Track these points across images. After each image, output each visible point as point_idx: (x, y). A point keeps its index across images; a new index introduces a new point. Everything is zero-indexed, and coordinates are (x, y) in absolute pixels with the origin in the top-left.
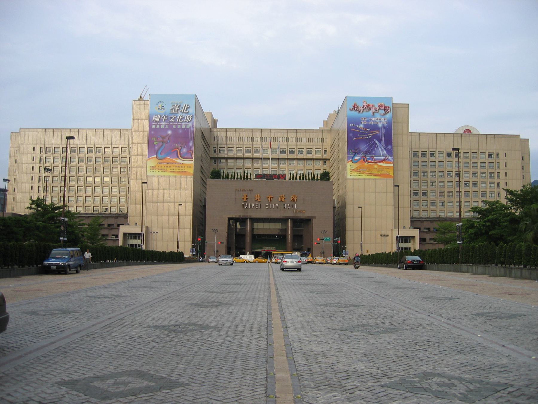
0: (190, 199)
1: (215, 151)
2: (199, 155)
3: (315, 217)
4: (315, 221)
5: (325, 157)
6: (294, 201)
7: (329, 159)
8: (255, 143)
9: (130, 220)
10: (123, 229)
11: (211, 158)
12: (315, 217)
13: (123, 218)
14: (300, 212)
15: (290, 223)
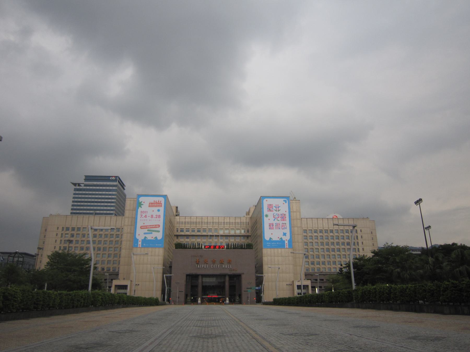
0: (161, 262)
1: (177, 231)
2: (168, 233)
3: (243, 274)
4: (243, 276)
5: (248, 234)
6: (229, 262)
7: (250, 236)
8: (203, 225)
9: (120, 276)
10: (115, 282)
11: (175, 235)
12: (243, 274)
13: (116, 275)
14: (234, 270)
15: (227, 278)
